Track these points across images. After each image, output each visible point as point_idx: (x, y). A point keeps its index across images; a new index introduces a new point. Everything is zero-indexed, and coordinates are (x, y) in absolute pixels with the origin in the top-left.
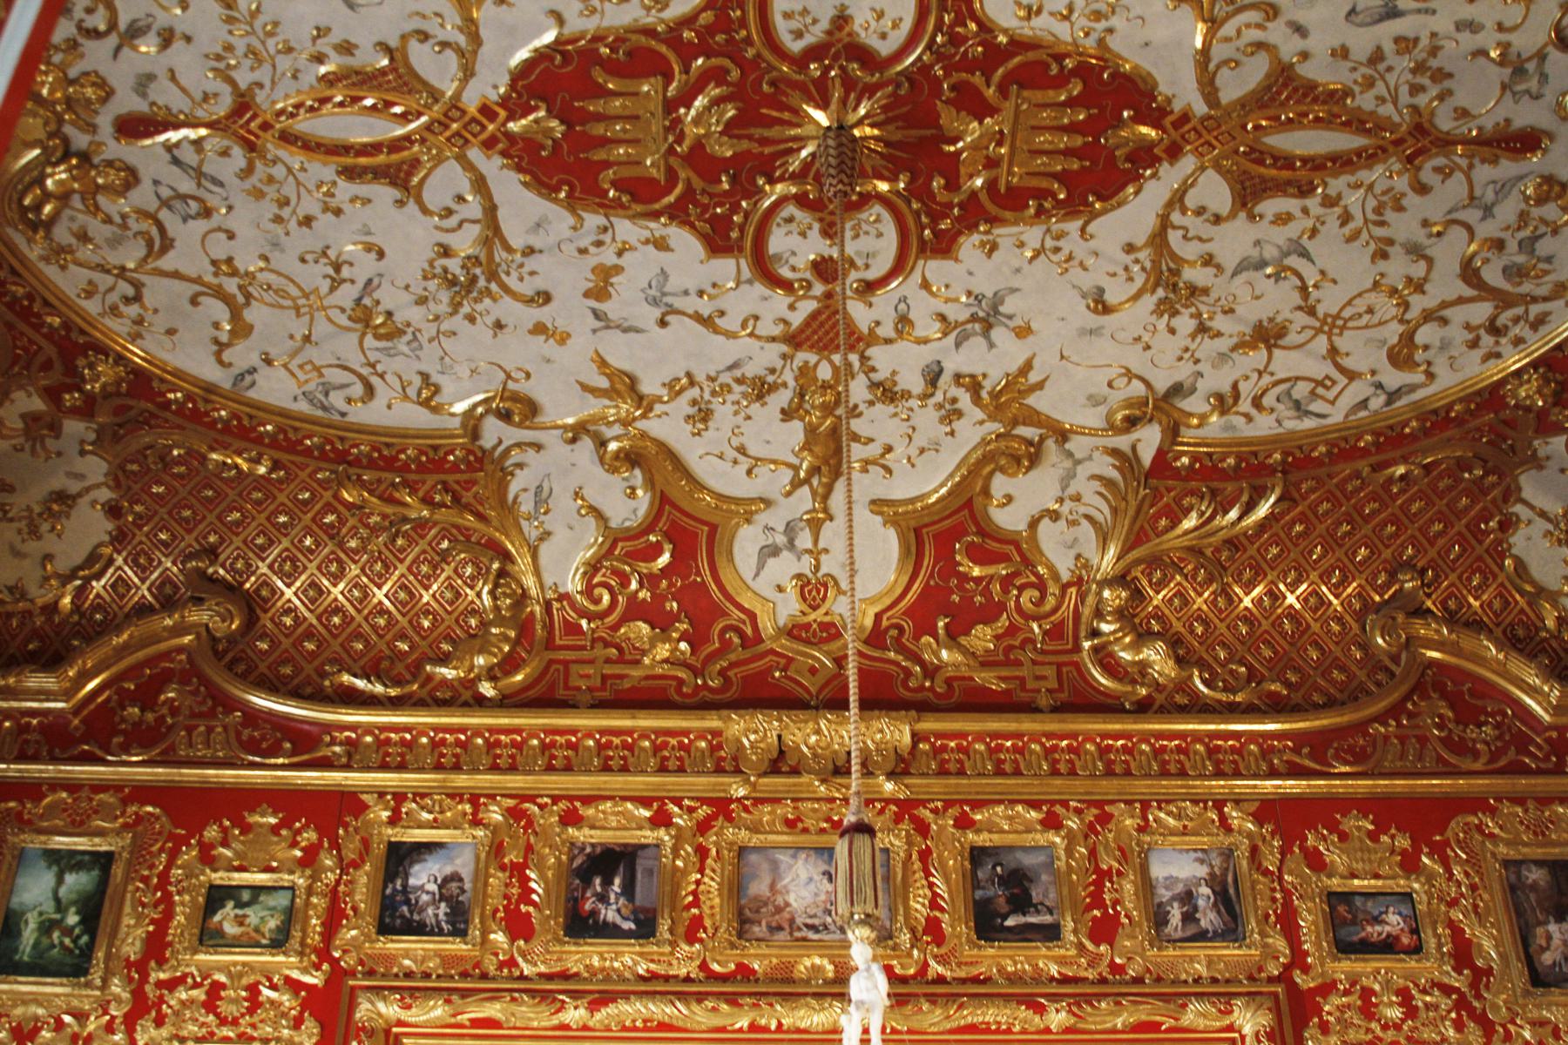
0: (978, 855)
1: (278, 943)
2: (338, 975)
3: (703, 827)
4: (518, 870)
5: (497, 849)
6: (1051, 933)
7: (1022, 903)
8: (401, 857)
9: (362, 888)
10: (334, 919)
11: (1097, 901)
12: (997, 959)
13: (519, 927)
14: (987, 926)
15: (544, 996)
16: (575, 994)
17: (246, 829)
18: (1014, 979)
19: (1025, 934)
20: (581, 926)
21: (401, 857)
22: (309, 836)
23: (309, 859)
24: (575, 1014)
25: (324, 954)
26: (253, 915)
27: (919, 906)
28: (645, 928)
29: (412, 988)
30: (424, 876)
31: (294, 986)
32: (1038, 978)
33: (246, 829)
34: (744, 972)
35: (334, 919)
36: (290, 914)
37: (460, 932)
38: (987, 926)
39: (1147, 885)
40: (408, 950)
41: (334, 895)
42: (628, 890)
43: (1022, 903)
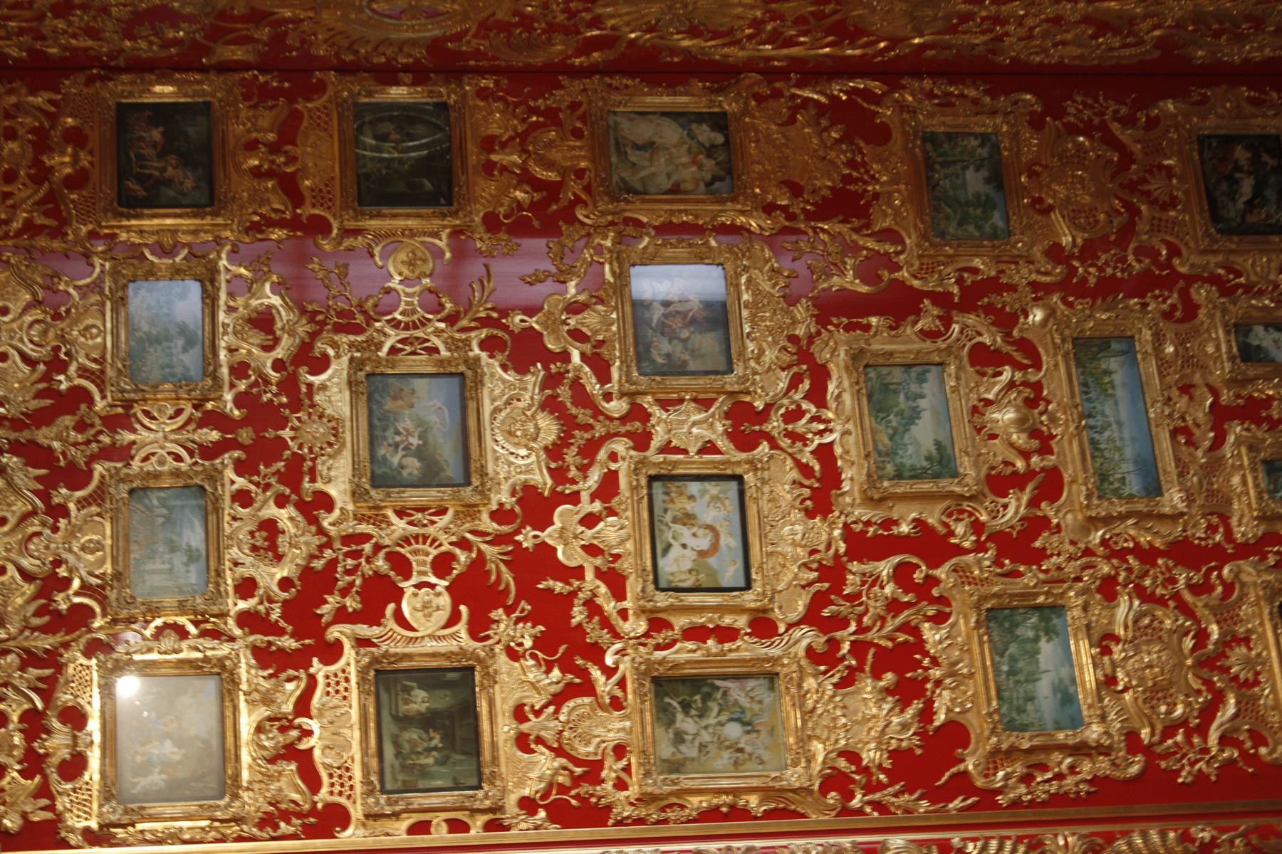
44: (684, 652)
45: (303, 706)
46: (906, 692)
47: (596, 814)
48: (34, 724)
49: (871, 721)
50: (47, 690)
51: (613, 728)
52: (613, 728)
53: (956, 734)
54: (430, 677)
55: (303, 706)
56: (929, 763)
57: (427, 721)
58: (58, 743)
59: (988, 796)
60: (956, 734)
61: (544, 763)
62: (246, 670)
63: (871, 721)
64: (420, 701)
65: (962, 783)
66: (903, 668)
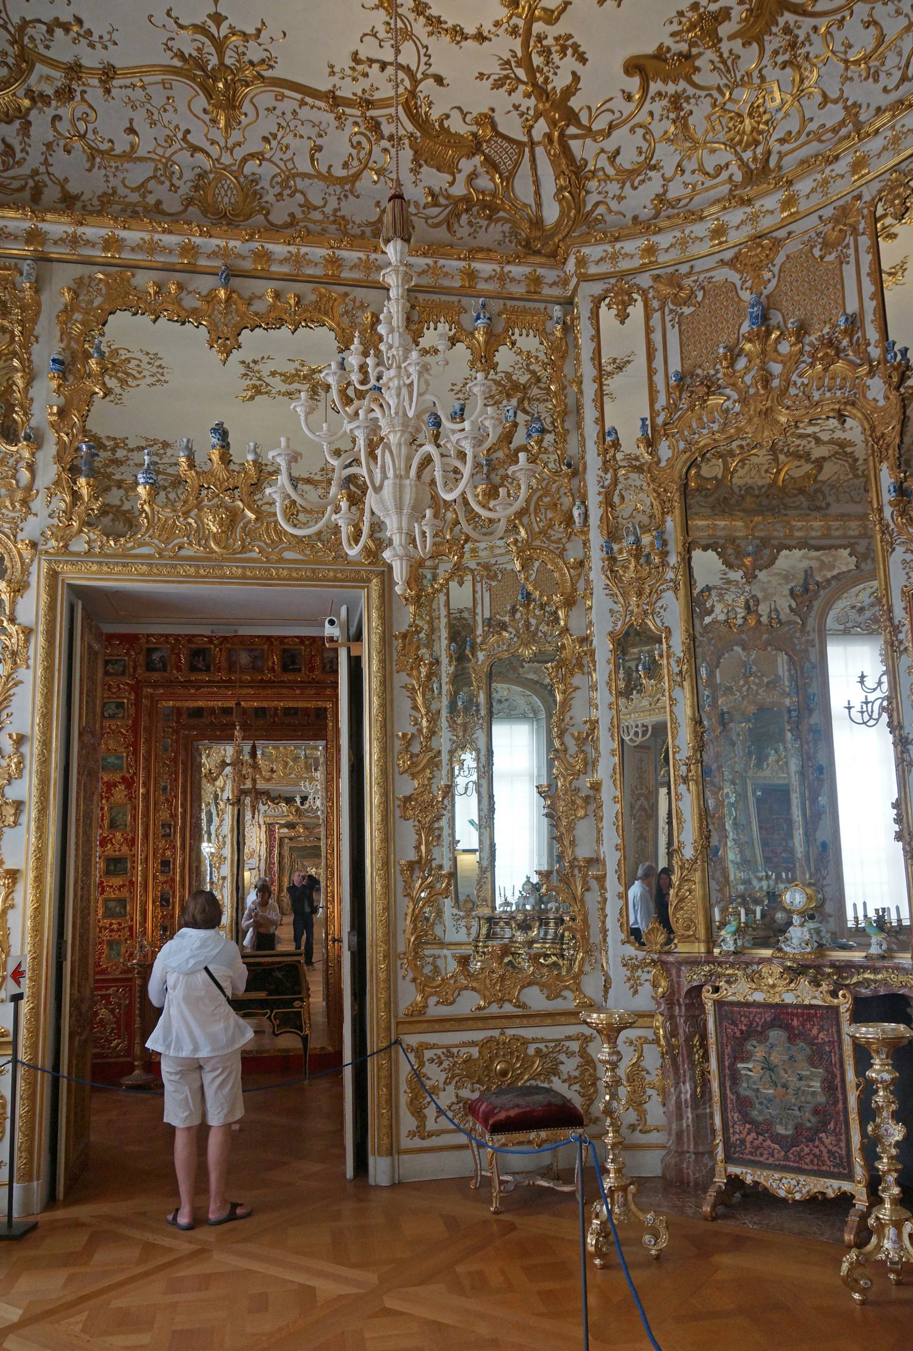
0: (284, 651)
1: (123, 673)
2: (138, 682)
3: (221, 643)
4: (178, 655)
5: (173, 649)
6: (299, 670)
7: (293, 663)
8: (150, 651)
9: (141, 659)
10: (135, 669)
11: (310, 662)
12: (287, 677)
13: (179, 669)
14: (285, 669)
15: (185, 687)
16: (193, 687)
17: (111, 645)
18: (290, 681)
19: (294, 670)
20: (193, 669)
21: (150, 651)
22: (127, 646)
23: (127, 653)
24: (193, 691)
25: (134, 677)
26: (116, 667)
27: (270, 664)
28: (208, 670)
29: (155, 686)
30: (156, 656)
31: (128, 684)
32: (296, 682)
33: (111, 645)
34: (230, 681)
35: (135, 669)
36: (125, 667)
37: (165, 670)
38: (285, 669)
39: (322, 659)
40: (155, 676)
41: (135, 662)
42: (204, 659)
43: (293, 663)
44: (106, 823)
45: (111, 887)
46: (115, 785)
47: (133, 839)
48: (112, 931)
49: (120, 793)
50: (106, 929)
51: (118, 835)
52: (118, 835)
53: (123, 778)
54: (108, 866)
55: (111, 887)
56: (129, 783)
57: (115, 866)
58: (115, 927)
59: (135, 774)
60: (123, 778)
61: (125, 848)
62: (106, 895)
63: (120, 793)
64: (112, 867)
65: (132, 778)
66: (110, 786)
